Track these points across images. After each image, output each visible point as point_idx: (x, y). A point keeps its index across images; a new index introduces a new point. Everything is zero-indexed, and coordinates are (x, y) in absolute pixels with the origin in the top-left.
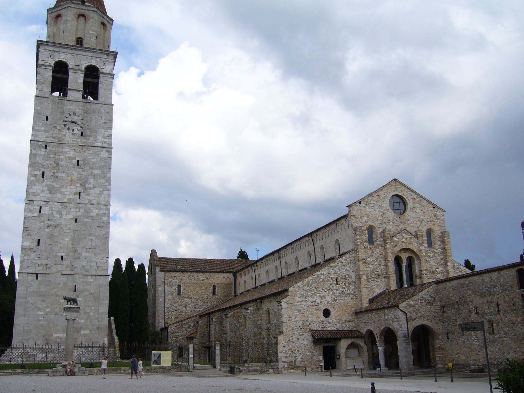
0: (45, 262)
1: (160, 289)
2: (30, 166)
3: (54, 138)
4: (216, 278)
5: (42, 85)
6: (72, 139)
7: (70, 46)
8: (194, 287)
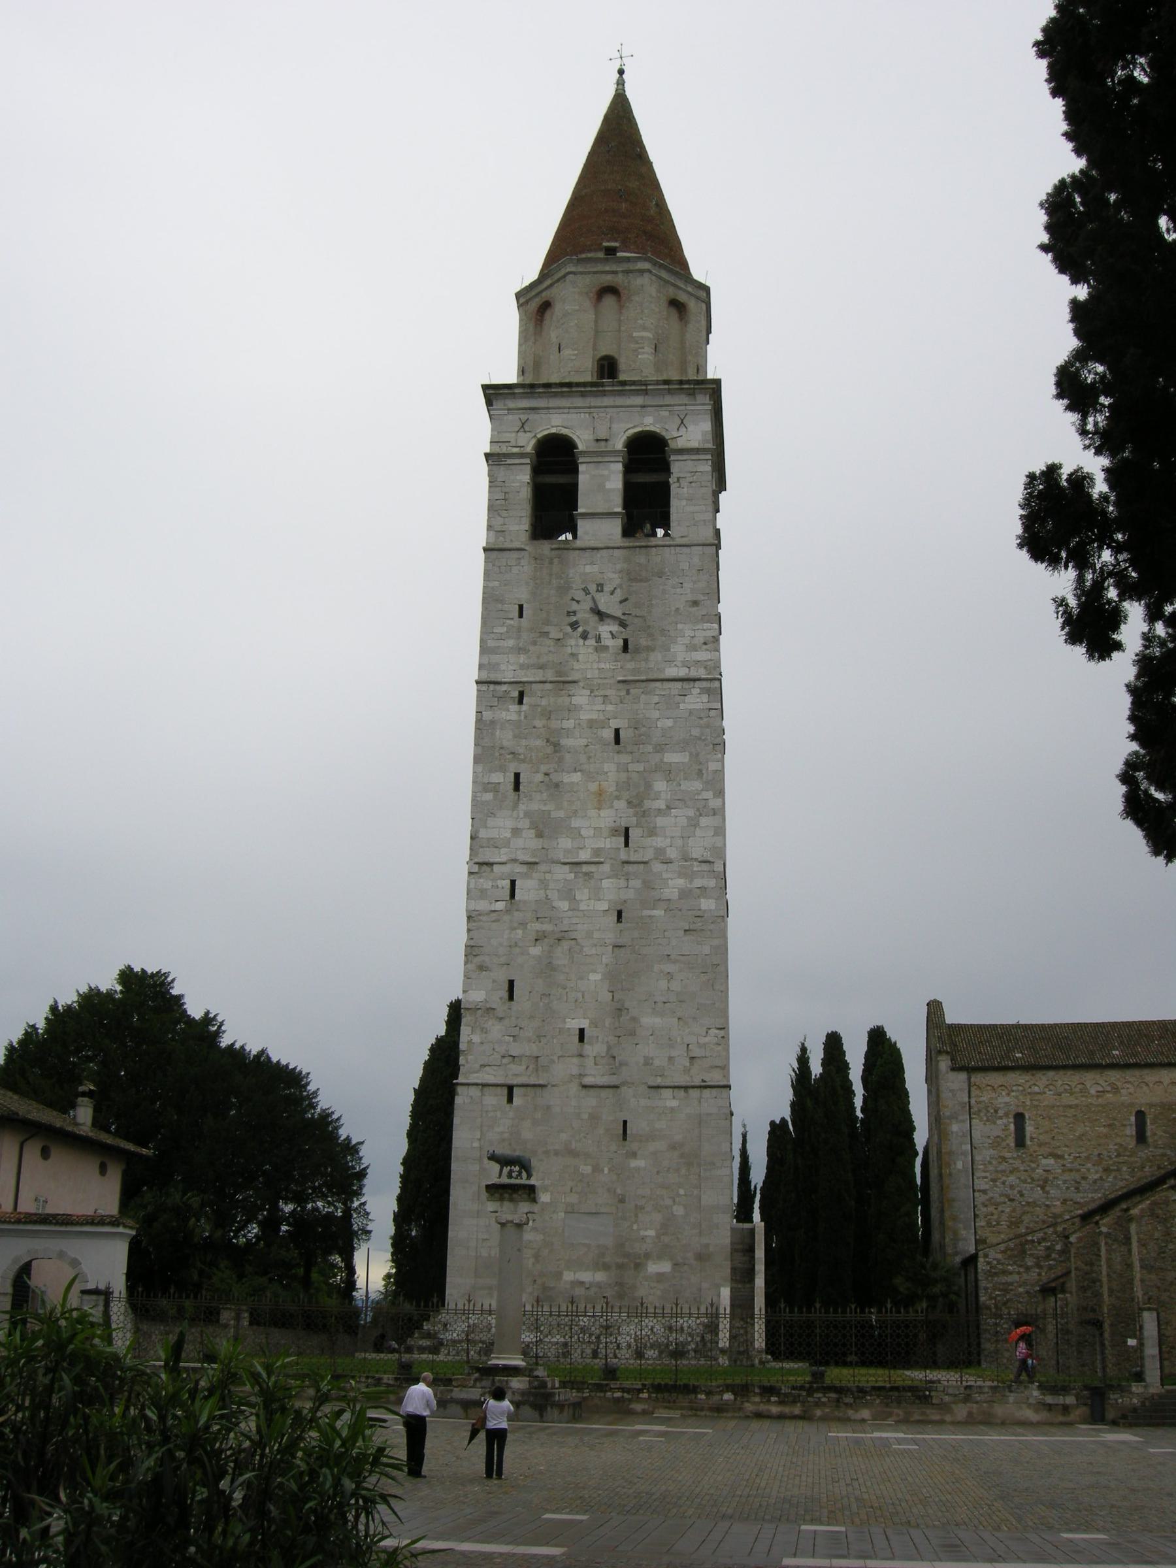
0: (532, 1049)
1: (955, 1127)
2: (477, 759)
3: (542, 667)
4: (1145, 1088)
5: (504, 514)
6: (595, 665)
7: (578, 385)
8: (1069, 1120)
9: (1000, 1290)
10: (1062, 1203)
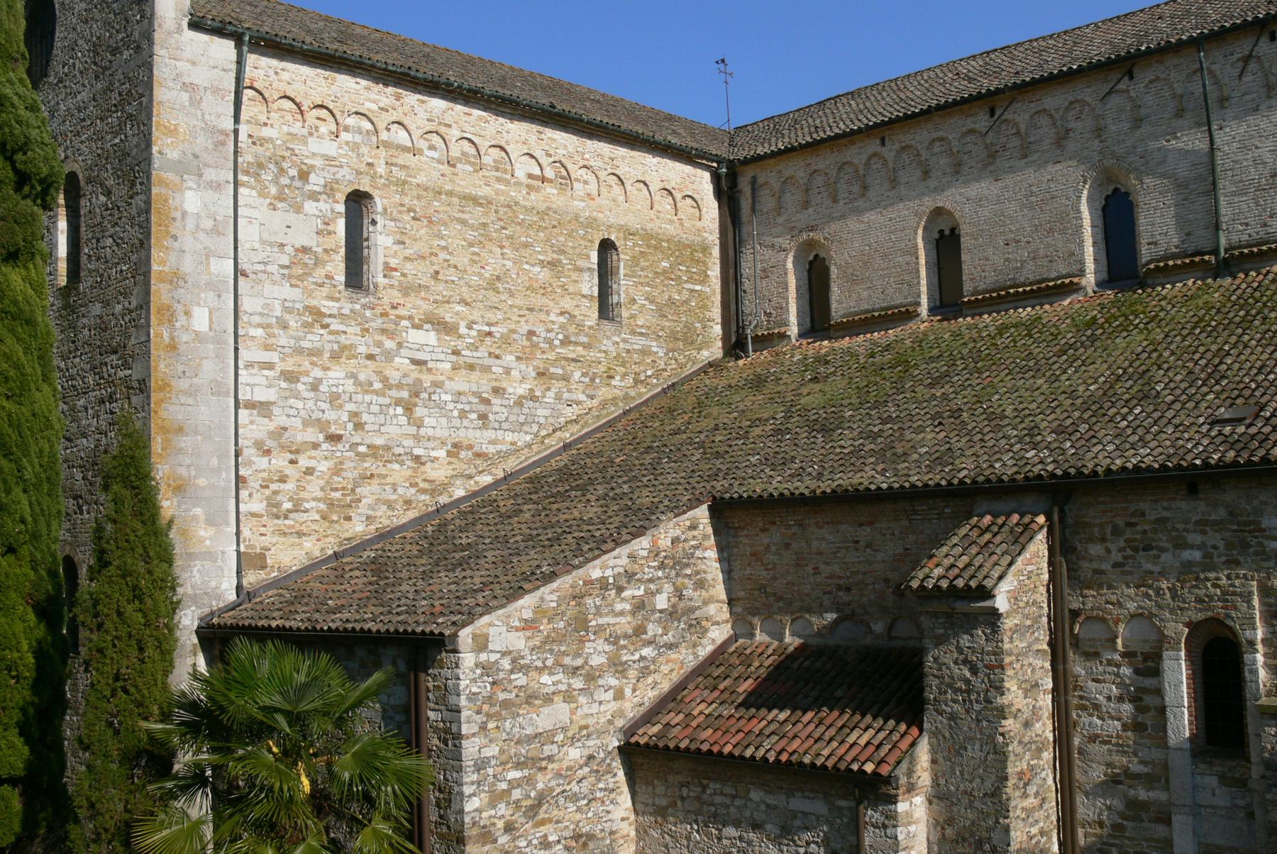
8: (471, 235)
9: (518, 766)
10: (449, 454)
